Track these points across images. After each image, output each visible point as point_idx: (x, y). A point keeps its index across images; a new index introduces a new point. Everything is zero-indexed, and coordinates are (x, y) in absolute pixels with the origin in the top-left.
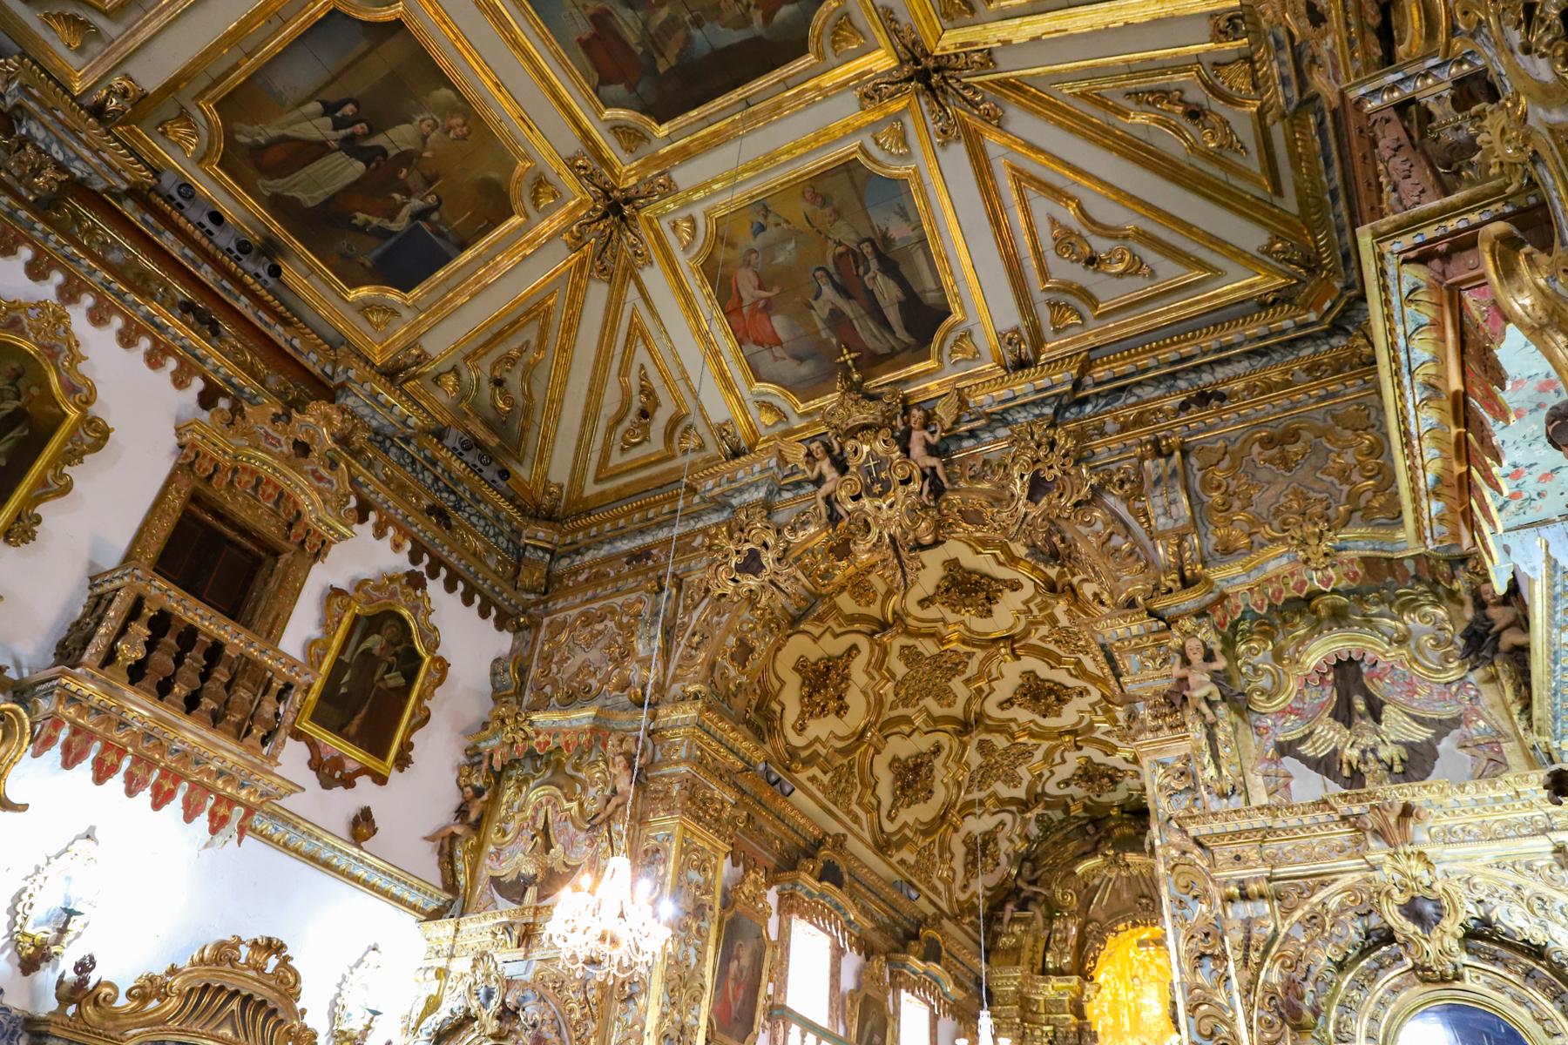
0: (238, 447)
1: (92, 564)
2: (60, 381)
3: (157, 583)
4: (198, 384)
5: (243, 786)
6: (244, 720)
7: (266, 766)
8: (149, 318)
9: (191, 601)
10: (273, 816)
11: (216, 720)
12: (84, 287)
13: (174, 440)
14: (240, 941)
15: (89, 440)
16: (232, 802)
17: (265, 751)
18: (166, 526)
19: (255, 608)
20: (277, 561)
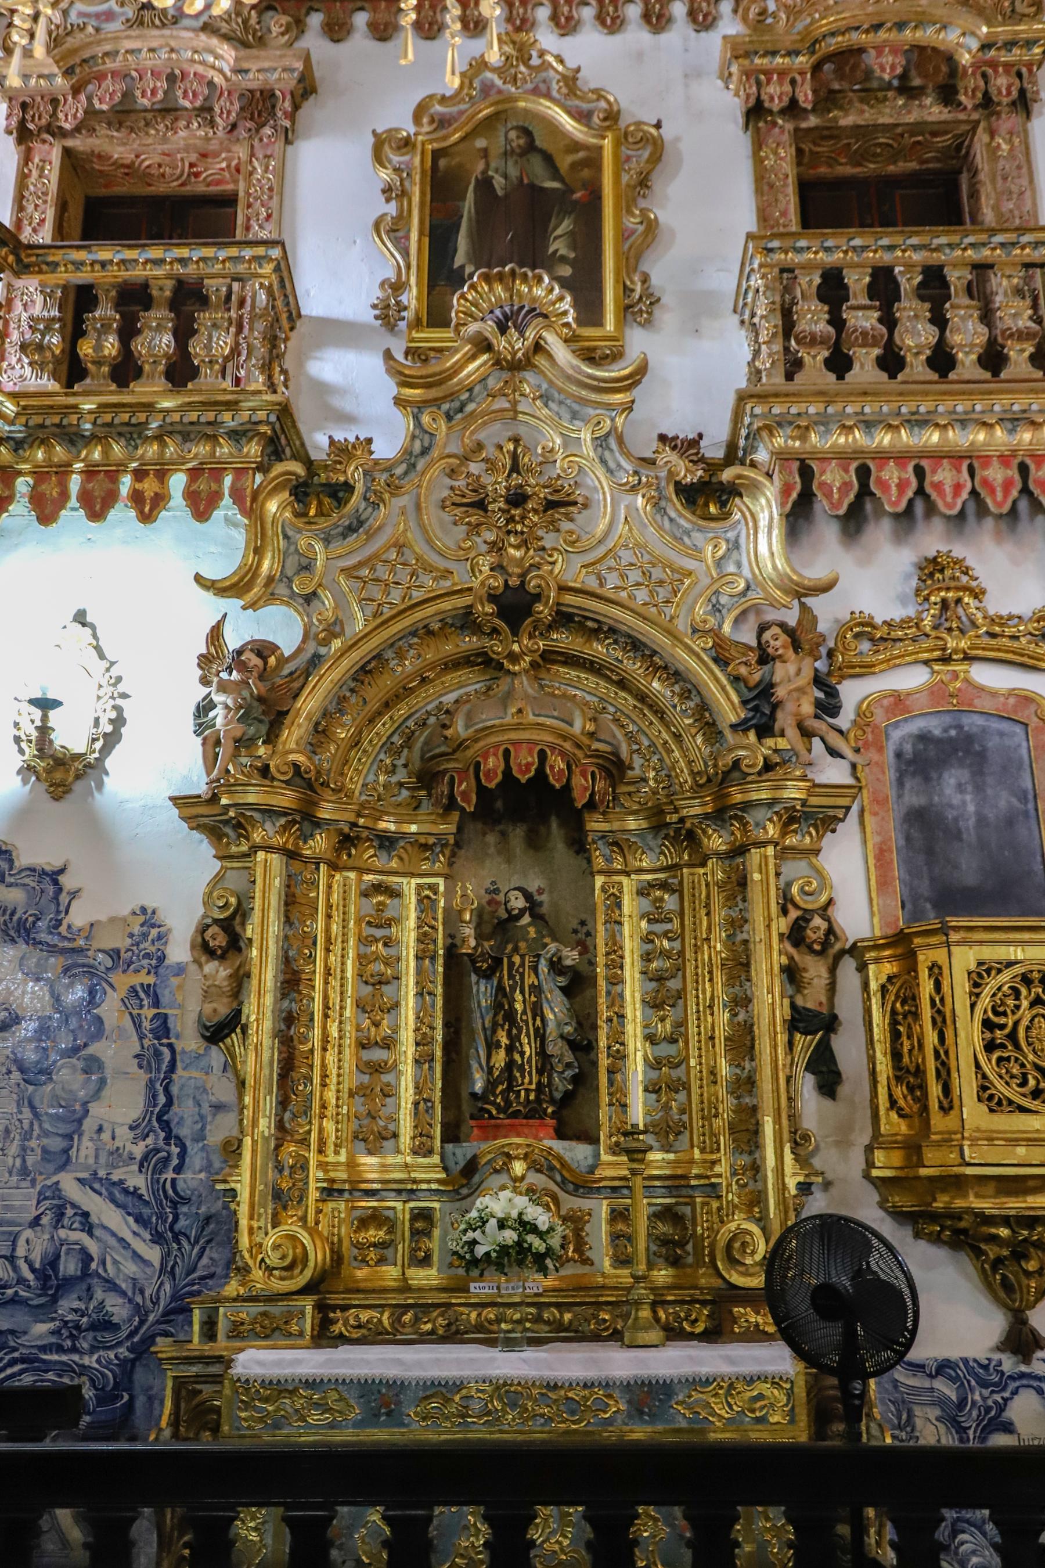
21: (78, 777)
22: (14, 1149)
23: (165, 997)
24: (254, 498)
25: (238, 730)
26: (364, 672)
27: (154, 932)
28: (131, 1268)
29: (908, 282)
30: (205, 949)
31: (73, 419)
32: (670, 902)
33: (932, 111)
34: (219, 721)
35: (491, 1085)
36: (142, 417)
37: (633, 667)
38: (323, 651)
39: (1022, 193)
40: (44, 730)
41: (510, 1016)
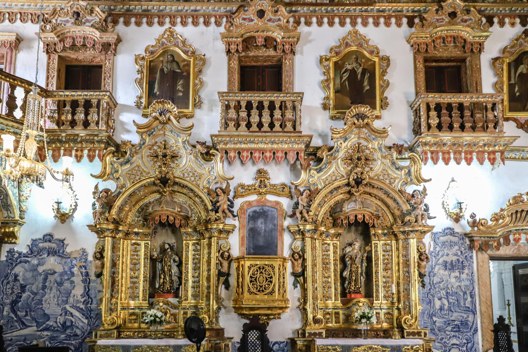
0: (430, 32)
1: (408, 102)
2: (367, 52)
3: (430, 96)
4: (405, 20)
5: (495, 146)
6: (484, 124)
7: (501, 135)
8: (379, 11)
9: (444, 95)
10: (512, 151)
11: (473, 128)
12: (356, 17)
13: (409, 45)
14: (521, 195)
15: (385, 65)
16: (494, 152)
17: (497, 130)
18: (422, 75)
19: (467, 84)
20: (466, 63)
21: (67, 218)
22: (56, 300)
23: (87, 268)
24: (103, 156)
25: (101, 210)
26: (130, 195)
27: (85, 254)
28: (81, 324)
29: (255, 105)
30: (95, 257)
31: (60, 138)
32: (198, 247)
33: (272, 52)
34: (97, 208)
35: (160, 286)
36: (76, 137)
37: (191, 194)
38: (121, 191)
39: (290, 76)
40: (58, 209)
41: (164, 272)
